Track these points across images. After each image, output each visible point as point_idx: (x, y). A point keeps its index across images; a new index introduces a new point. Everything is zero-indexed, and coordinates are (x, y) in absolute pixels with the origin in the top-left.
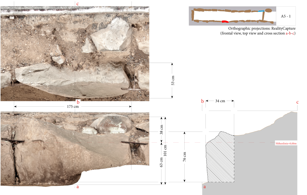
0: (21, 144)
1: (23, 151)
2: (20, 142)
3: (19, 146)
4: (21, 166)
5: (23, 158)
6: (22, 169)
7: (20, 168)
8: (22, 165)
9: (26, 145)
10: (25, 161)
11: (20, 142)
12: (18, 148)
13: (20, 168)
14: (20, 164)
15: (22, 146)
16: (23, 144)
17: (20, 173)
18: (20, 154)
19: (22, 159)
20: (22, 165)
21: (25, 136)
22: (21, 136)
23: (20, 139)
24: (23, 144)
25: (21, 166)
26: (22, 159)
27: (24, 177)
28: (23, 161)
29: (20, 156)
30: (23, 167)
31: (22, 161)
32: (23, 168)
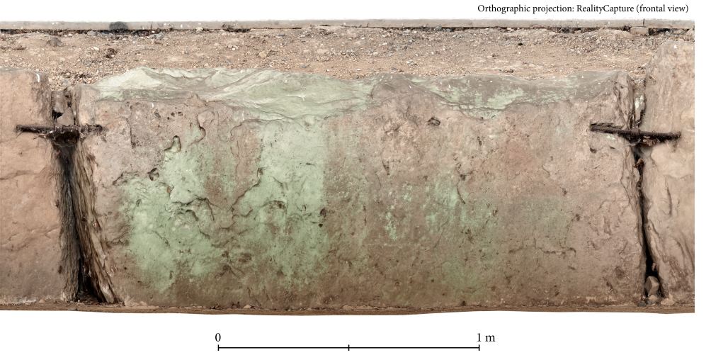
0: (667, 146)
2: (662, 138)
3: (659, 153)
4: (669, 232)
6: (671, 242)
7: (663, 241)
11: (662, 138)
13: (663, 241)
14: (665, 225)
17: (665, 262)
18: (663, 185)
19: (671, 206)
22: (667, 117)
23: (665, 129)
25: (669, 232)
26: (671, 206)
31: (670, 213)
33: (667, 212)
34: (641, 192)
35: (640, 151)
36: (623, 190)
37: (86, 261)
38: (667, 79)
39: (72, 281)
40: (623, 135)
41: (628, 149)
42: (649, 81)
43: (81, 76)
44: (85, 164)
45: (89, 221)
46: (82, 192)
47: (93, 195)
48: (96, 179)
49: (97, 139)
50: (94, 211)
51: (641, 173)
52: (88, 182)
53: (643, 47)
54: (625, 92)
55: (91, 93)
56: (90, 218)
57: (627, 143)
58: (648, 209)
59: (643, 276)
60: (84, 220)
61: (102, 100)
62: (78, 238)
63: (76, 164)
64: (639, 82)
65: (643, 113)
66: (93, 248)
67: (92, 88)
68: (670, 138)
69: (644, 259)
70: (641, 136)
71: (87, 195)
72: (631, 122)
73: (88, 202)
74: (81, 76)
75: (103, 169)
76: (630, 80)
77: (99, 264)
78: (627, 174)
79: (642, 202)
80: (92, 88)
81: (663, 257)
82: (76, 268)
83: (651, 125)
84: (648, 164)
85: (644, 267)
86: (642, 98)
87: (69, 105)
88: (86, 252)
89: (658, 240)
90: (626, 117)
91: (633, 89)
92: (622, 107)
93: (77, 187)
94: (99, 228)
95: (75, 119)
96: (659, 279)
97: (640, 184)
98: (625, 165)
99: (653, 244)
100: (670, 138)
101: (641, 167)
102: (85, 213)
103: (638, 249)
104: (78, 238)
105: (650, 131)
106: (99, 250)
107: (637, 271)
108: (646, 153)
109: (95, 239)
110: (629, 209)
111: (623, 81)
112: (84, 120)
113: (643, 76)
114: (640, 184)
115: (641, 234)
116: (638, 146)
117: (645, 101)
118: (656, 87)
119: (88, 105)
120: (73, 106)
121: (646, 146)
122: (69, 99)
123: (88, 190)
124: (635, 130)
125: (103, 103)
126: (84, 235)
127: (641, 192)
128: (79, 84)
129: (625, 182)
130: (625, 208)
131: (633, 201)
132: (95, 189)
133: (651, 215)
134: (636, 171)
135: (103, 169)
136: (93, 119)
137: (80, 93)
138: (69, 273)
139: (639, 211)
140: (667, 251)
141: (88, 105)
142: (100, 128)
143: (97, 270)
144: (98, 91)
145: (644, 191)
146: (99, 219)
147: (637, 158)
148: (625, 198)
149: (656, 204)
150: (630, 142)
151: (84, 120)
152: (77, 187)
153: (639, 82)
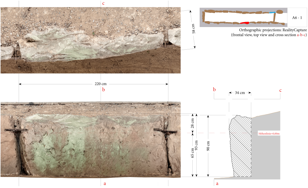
0: (174, 134)
1: (175, 142)
2: (172, 132)
3: (171, 136)
4: (174, 157)
5: (175, 149)
6: (174, 159)
7: (172, 159)
8: (175, 156)
9: (178, 135)
10: (178, 152)
11: (172, 132)
12: (171, 138)
13: (172, 159)
14: (173, 155)
15: (175, 137)
16: (176, 134)
17: (173, 164)
18: (172, 144)
19: (174, 150)
20: (175, 156)
21: (178, 127)
22: (174, 127)
23: (173, 130)
24: (176, 134)
25: (174, 157)
26: (174, 150)
27: (177, 168)
28: (175, 151)
29: (173, 147)
30: (176, 157)
31: (174, 152)
32: (175, 159)
33: (174, 151)
34: (167, 146)
35: (166, 136)
36: (162, 146)
37: (23, 164)
38: (174, 117)
39: (19, 169)
40: (162, 131)
41: (163, 135)
42: (169, 118)
43: (22, 116)
44: (23, 139)
45: (24, 154)
46: (22, 146)
47: (25, 147)
48: (25, 143)
49: (26, 132)
50: (25, 151)
51: (167, 141)
52: (24, 144)
53: (167, 109)
54: (163, 120)
55: (24, 121)
56: (24, 153)
57: (163, 134)
58: (168, 151)
59: (167, 168)
60: (22, 154)
61: (27, 122)
62: (21, 158)
63: (20, 139)
64: (166, 118)
65: (167, 126)
66: (25, 161)
67: (24, 119)
68: (175, 132)
69: (168, 164)
70: (167, 132)
71: (23, 147)
72: (164, 128)
73: (23, 149)
74: (22, 116)
75: (27, 140)
76: (164, 117)
77: (26, 165)
78: (163, 142)
79: (167, 149)
80: (24, 119)
81: (173, 163)
82: (20, 166)
83: (170, 129)
84: (169, 139)
85: (168, 166)
86: (167, 122)
87: (19, 124)
88: (23, 162)
89: (171, 159)
90: (163, 127)
91: (165, 119)
92: (162, 124)
93: (21, 145)
94: (26, 156)
95: (20, 127)
96: (171, 169)
97: (166, 144)
98: (163, 139)
99: (170, 160)
100: (175, 132)
101: (167, 140)
102: (23, 152)
103: (166, 161)
104: (21, 158)
105: (169, 130)
106: (26, 161)
107: (166, 167)
108: (168, 137)
109: (25, 158)
110: (164, 151)
111: (162, 117)
112: (22, 128)
113: (167, 116)
114: (166, 144)
115: (167, 157)
116: (166, 134)
117: (168, 123)
118: (171, 119)
119: (24, 124)
120: (20, 124)
121: (168, 134)
122: (18, 122)
123: (23, 146)
124: (165, 130)
125: (27, 123)
126: (22, 157)
127: (167, 146)
128: (21, 118)
129: (163, 144)
130: (162, 150)
131: (165, 149)
132: (25, 146)
133: (169, 152)
134: (165, 141)
135: (27, 140)
136: (25, 127)
137: (21, 121)
138: (18, 167)
139: (166, 151)
140: (174, 162)
141: (24, 124)
142: (26, 130)
143: (26, 166)
144: (26, 120)
145: (168, 146)
146: (26, 153)
147: (166, 137)
148: (163, 148)
149: (171, 149)
150: (164, 133)
151: (22, 128)
152: (21, 145)
153: (166, 118)
